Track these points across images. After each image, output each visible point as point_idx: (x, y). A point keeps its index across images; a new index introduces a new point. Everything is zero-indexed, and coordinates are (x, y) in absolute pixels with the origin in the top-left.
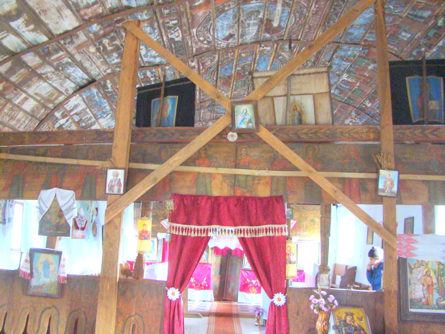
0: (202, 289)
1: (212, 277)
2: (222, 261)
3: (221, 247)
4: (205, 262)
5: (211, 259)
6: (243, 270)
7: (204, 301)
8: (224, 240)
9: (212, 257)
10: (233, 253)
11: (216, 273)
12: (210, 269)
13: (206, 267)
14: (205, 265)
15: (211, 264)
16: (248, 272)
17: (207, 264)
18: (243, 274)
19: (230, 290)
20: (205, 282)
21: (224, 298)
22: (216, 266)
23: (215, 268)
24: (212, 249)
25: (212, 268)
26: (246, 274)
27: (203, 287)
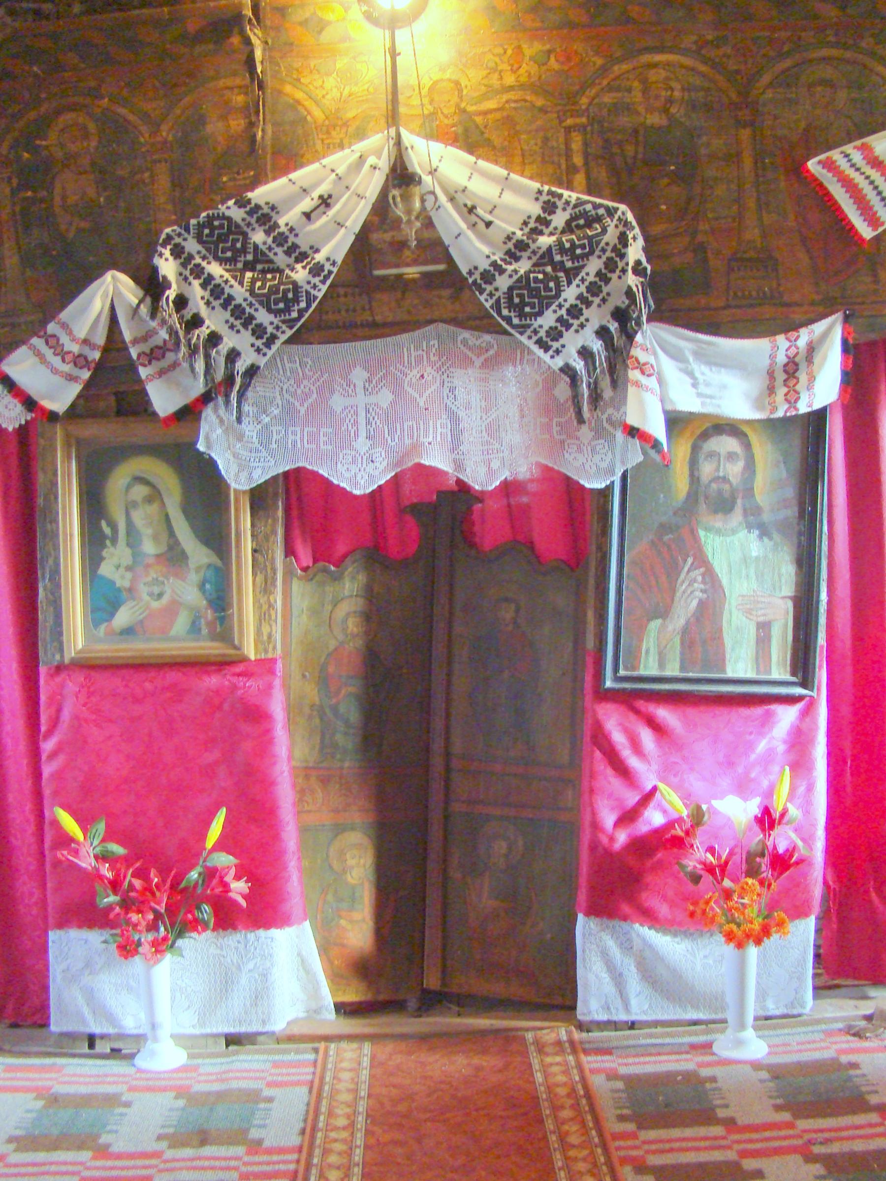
0: (195, 925)
1: (285, 794)
2: (374, 612)
3: (359, 472)
4: (206, 647)
5: (264, 616)
6: (604, 696)
7: (232, 1040)
8: (385, 398)
9: (266, 588)
10: (491, 531)
11: (327, 748)
12: (257, 715)
13: (214, 703)
14: (213, 681)
15: (267, 666)
16: (663, 713)
17: (221, 665)
18: (618, 738)
19: (483, 898)
20: (224, 860)
21: (432, 981)
22: (324, 680)
23: (312, 693)
24: (259, 498)
25: (277, 708)
26: (647, 737)
27: (206, 912)
